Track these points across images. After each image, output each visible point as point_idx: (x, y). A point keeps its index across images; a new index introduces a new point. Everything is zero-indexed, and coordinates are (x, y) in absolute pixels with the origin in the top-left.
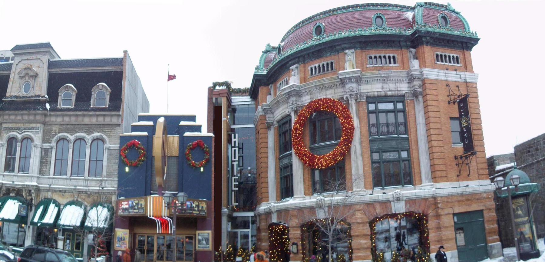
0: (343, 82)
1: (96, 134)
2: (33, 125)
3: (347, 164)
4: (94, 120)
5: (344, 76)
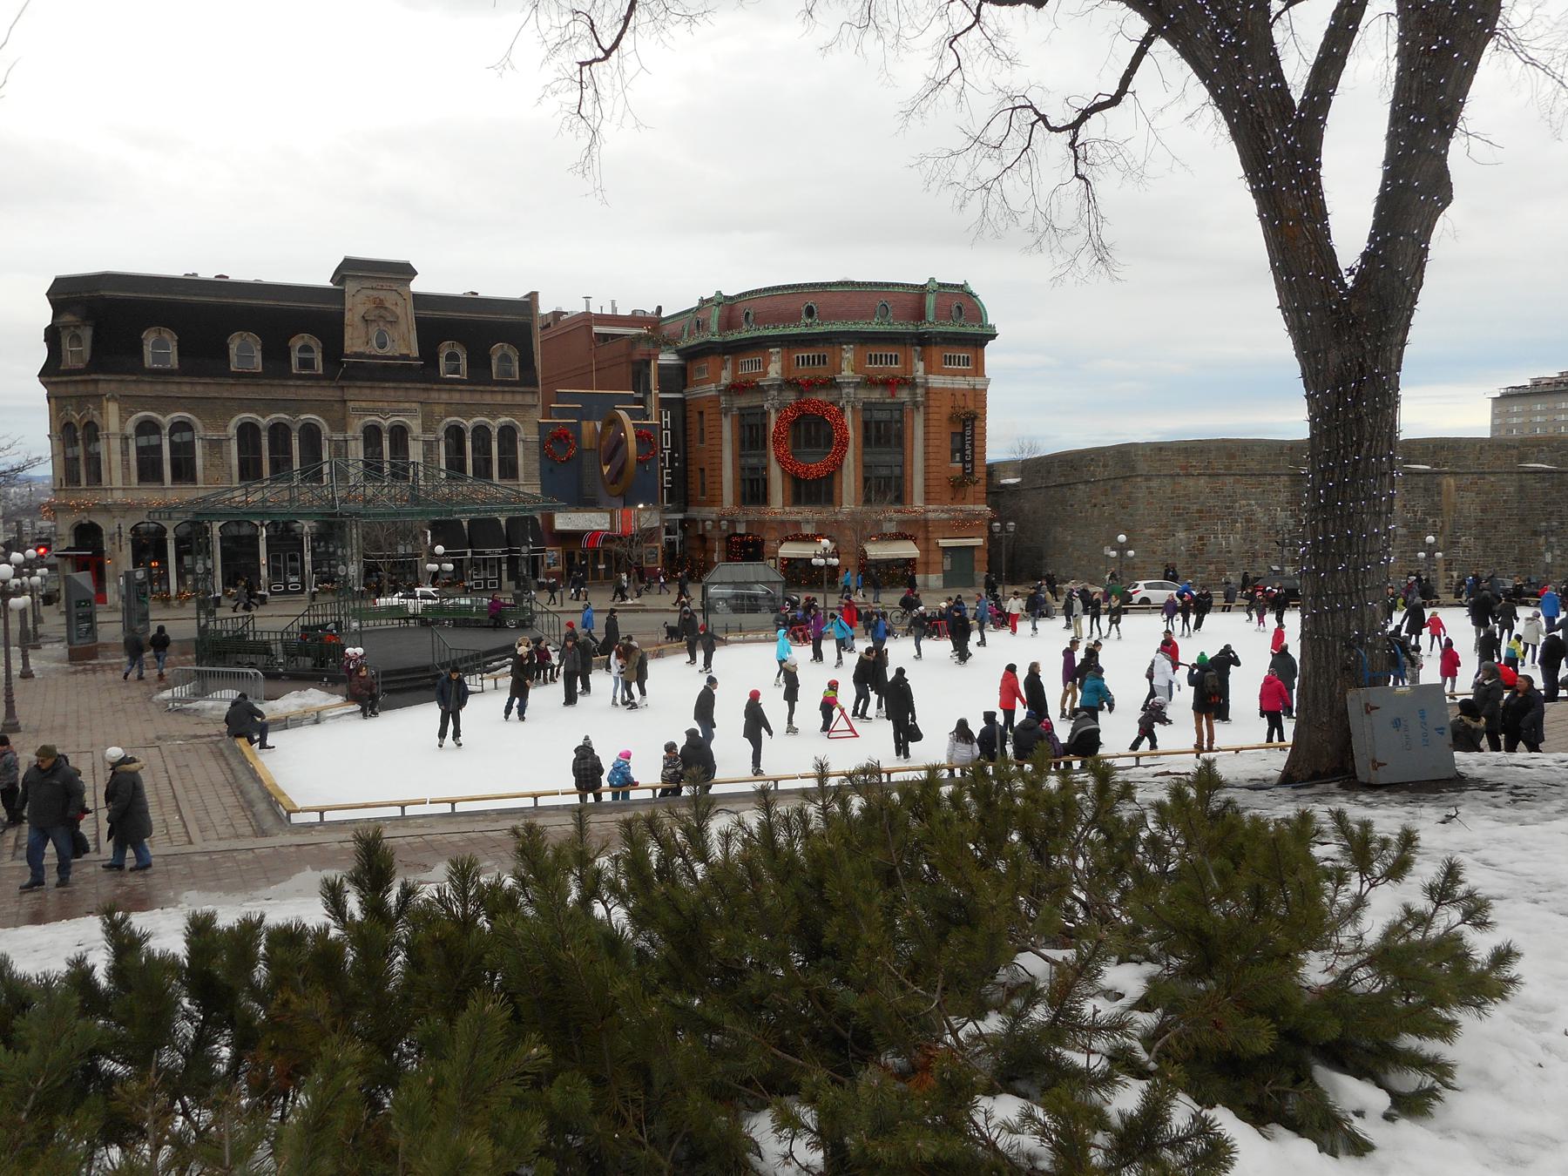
1: (504, 420)
2: (407, 405)
3: (837, 479)
4: (499, 399)
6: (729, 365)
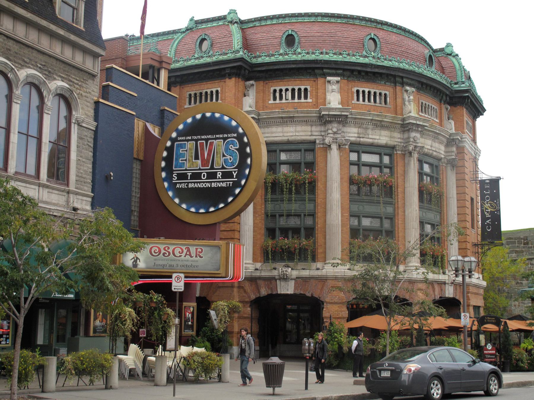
0: (406, 127)
5: (415, 122)
6: (252, 93)
